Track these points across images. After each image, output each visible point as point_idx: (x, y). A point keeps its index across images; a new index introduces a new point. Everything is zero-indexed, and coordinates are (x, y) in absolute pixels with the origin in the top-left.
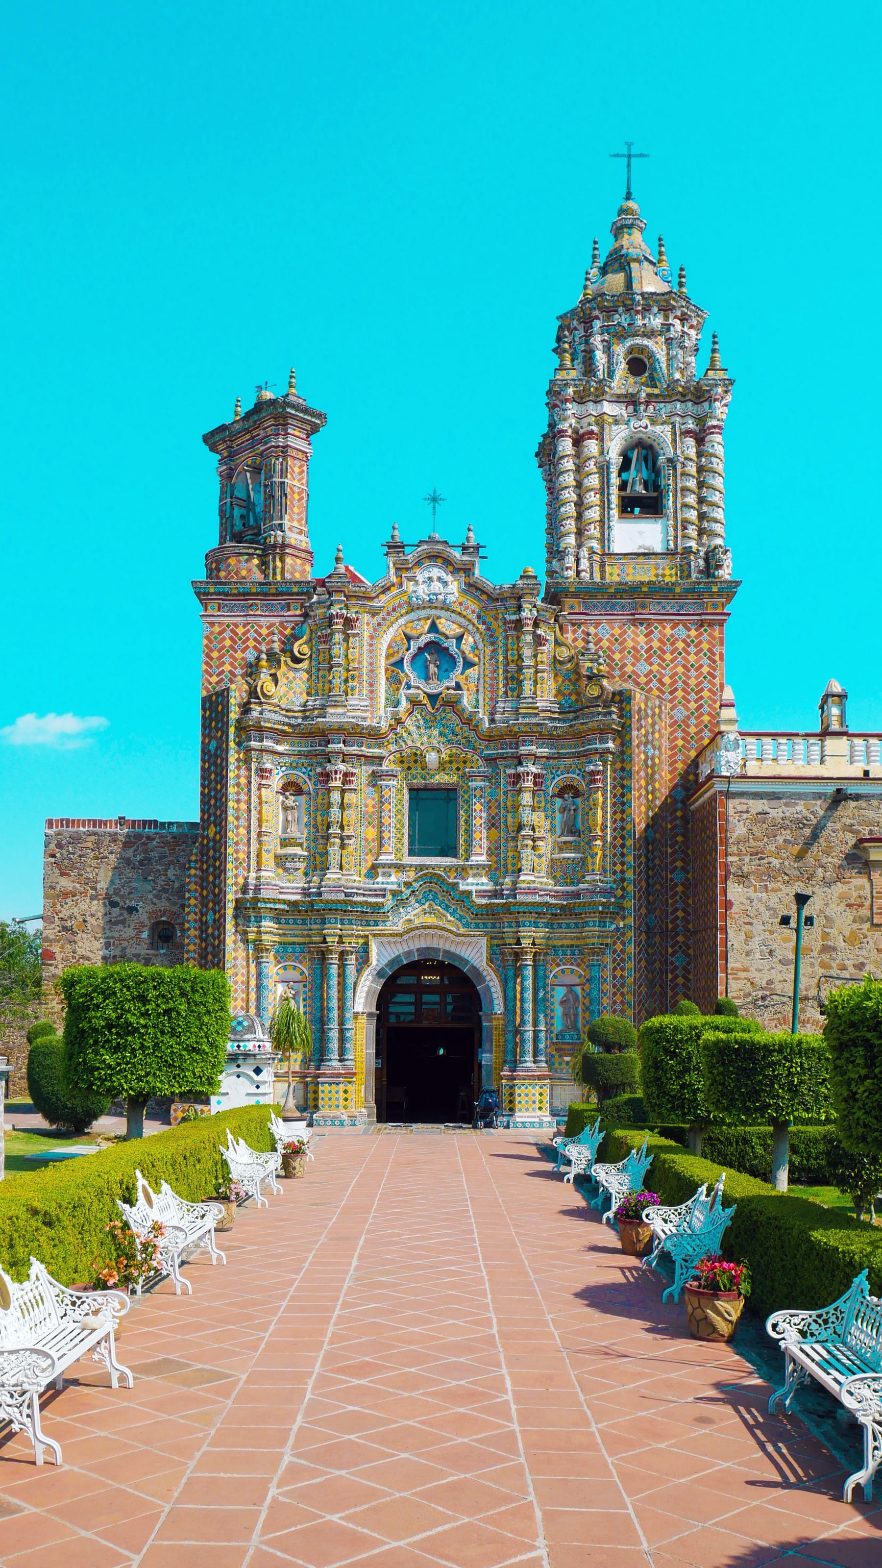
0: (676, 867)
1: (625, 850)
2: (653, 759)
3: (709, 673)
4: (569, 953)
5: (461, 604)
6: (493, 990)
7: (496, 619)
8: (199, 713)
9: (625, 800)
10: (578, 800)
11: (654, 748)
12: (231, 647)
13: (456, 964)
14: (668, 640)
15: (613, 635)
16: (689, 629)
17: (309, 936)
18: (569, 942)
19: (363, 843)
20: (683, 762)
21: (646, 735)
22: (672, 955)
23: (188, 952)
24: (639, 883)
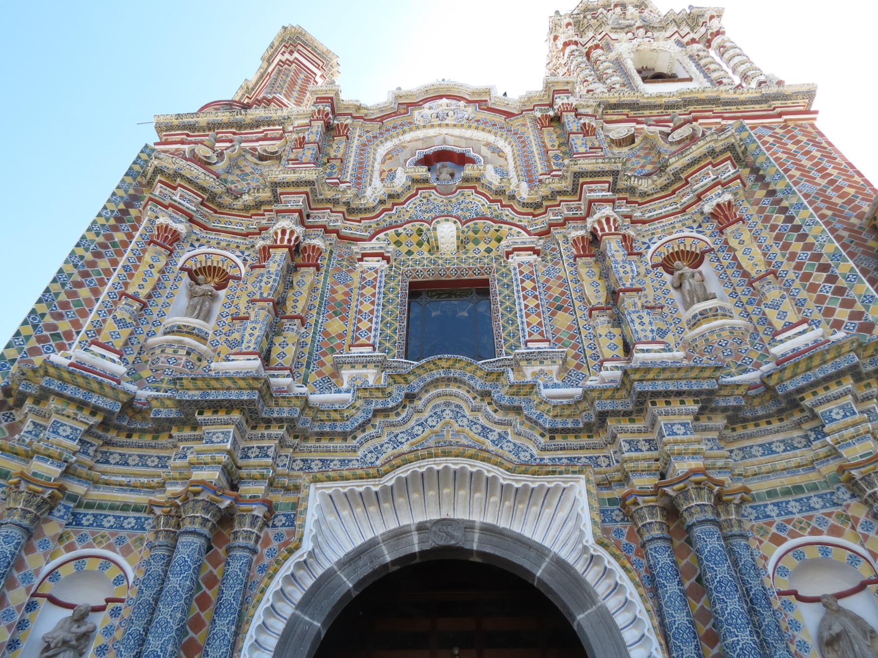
4: (794, 507)
5: (478, 121)
6: (621, 619)
7: (524, 125)
9: (797, 221)
13: (517, 558)
16: (774, 129)
20: (845, 229)
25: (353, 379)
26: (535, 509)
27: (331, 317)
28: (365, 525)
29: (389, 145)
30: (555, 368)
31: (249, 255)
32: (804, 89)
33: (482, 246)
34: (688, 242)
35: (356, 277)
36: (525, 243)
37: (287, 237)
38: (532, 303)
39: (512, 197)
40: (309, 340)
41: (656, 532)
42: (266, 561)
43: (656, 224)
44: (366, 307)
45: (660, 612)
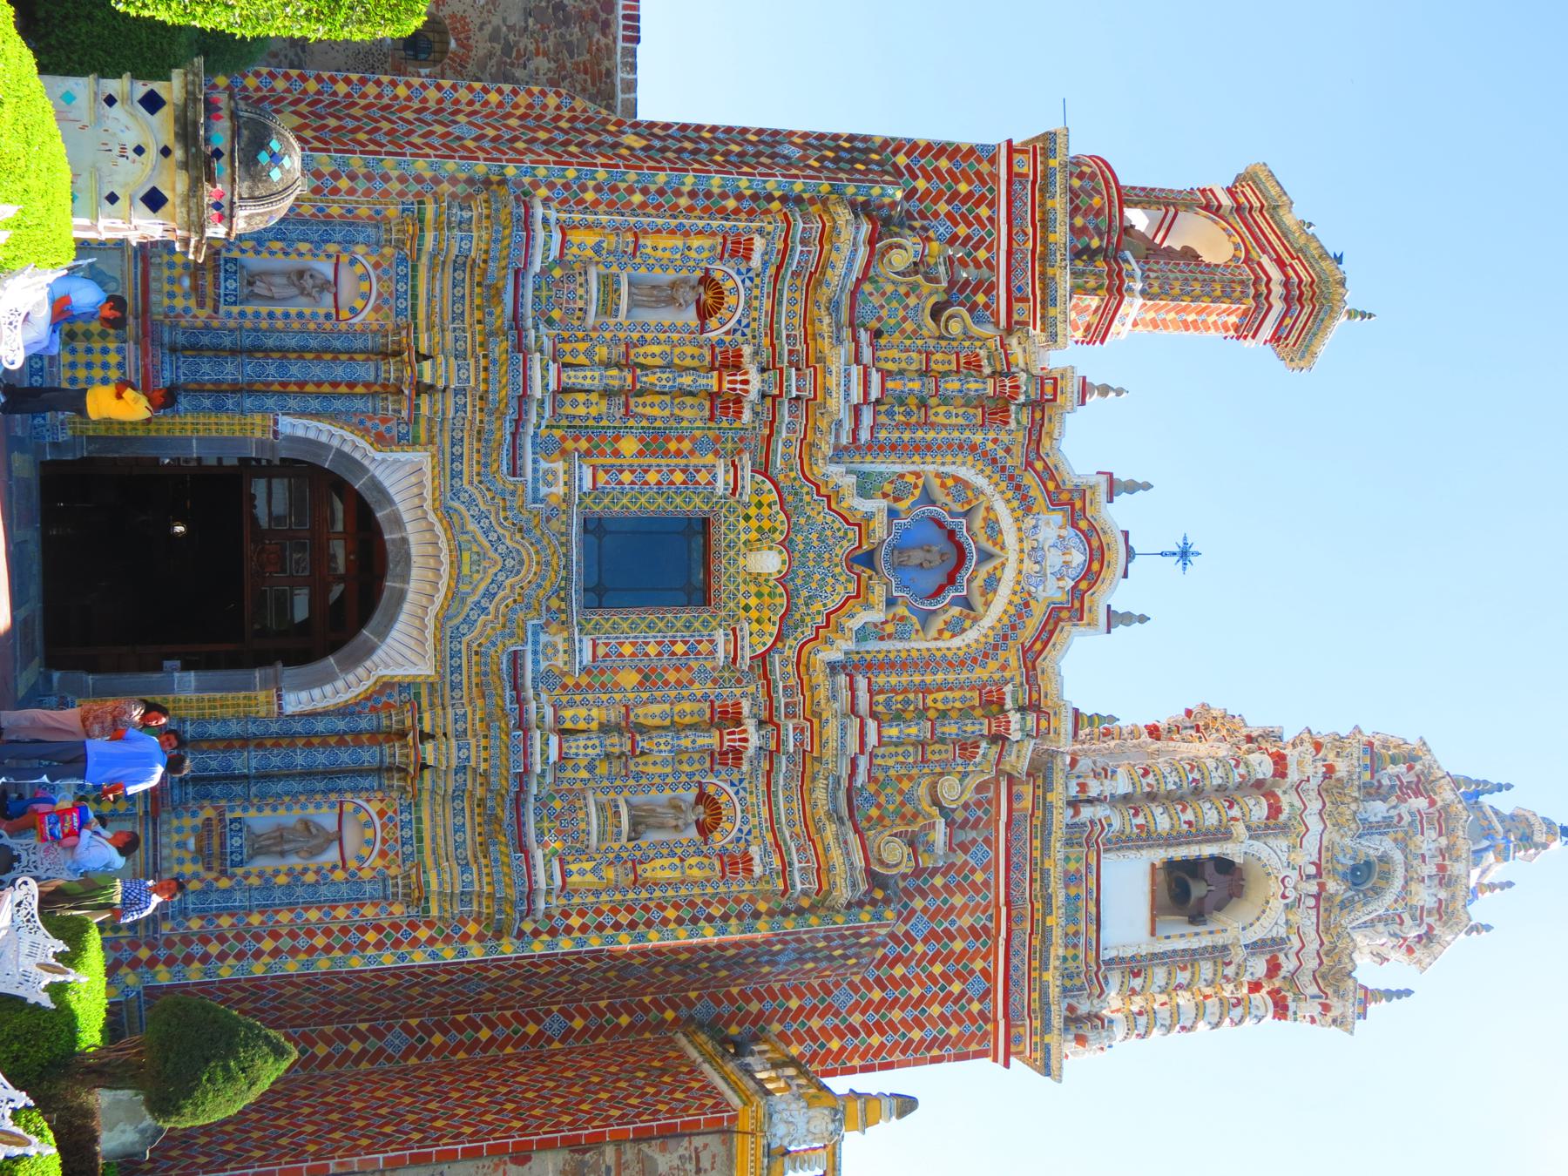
0: (572, 1018)
1: (609, 931)
2: (769, 963)
3: (911, 1041)
4: (407, 833)
5: (1027, 605)
6: (328, 689)
7: (1003, 668)
8: (845, 129)
9: (702, 923)
10: (693, 832)
11: (787, 964)
12: (956, 194)
13: (377, 617)
14: (965, 966)
15: (973, 871)
16: (981, 1000)
17: (430, 328)
18: (427, 835)
19: (610, 432)
20: (761, 1013)
21: (813, 949)
22: (407, 1028)
23: (394, 84)
24: (549, 963)
25: (554, 473)
26: (415, 633)
27: (641, 440)
28: (405, 495)
29: (980, 481)
30: (561, 664)
31: (744, 334)
32: (1054, 1063)
33: (753, 602)
34: (728, 826)
35: (710, 458)
36: (742, 648)
37: (738, 386)
38: (652, 650)
39: (829, 642)
40: (604, 423)
41: (385, 722)
42: (369, 424)
43: (762, 798)
44: (652, 477)
45: (325, 713)
